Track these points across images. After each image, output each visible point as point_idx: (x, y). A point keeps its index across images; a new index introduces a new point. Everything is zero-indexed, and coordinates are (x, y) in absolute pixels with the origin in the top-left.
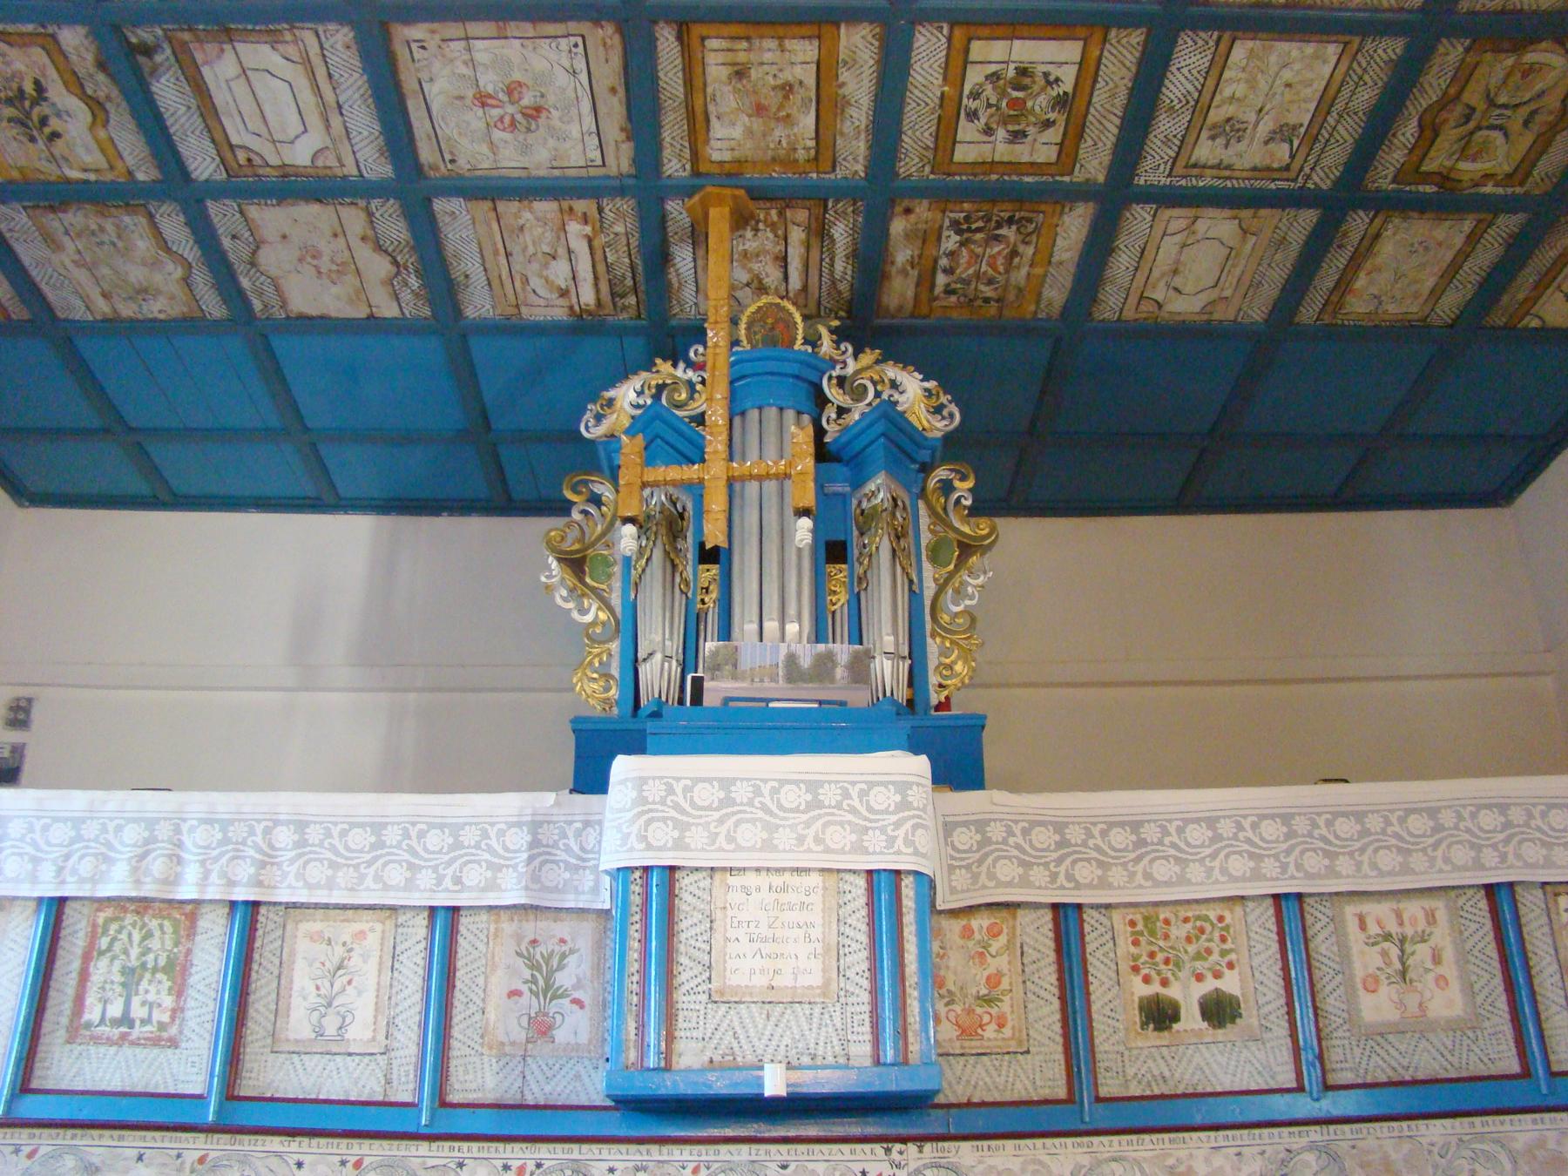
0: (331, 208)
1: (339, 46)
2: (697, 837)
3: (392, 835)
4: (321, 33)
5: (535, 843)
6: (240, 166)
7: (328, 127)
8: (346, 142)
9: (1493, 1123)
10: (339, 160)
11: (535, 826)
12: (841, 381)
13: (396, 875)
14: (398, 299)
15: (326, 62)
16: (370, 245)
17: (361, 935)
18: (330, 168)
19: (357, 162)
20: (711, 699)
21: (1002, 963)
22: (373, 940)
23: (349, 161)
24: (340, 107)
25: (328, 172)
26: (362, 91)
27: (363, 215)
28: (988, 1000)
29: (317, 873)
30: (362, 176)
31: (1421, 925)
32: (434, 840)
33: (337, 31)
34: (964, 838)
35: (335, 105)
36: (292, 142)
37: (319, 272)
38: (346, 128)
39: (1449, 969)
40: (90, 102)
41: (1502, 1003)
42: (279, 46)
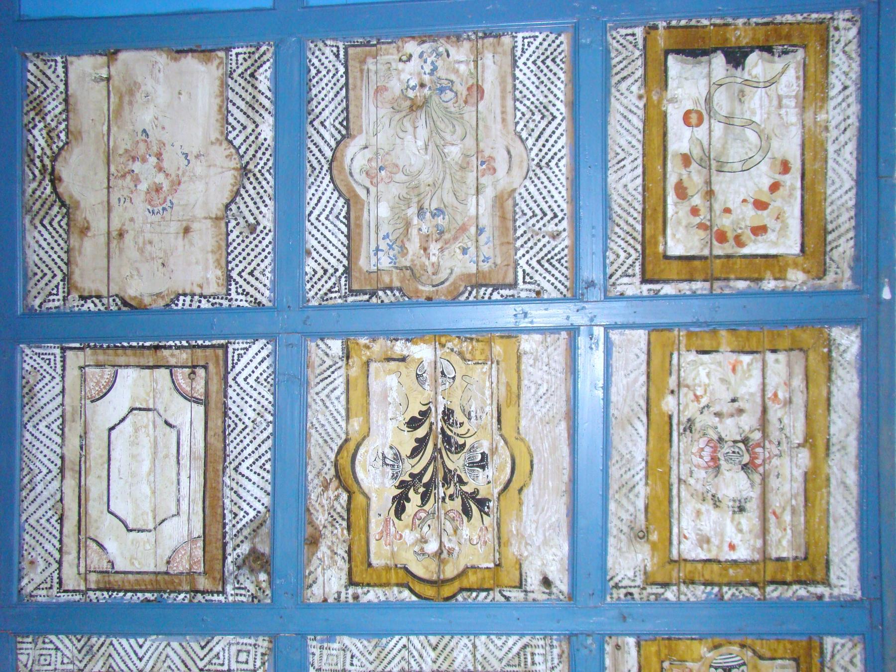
0: (114, 290)
1: (42, 565)
4: (56, 586)
6: (205, 367)
7: (84, 436)
8: (68, 408)
10: (84, 379)
14: (66, 101)
15: (61, 541)
16: (79, 216)
18: (99, 365)
19: (63, 377)
23: (73, 374)
24: (62, 470)
25: (101, 358)
26: (32, 495)
27: (76, 277)
30: (64, 350)
33: (37, 588)
35: (68, 474)
36: (132, 409)
37: (159, 156)
38: (63, 436)
40: (351, 481)
42: (105, 566)
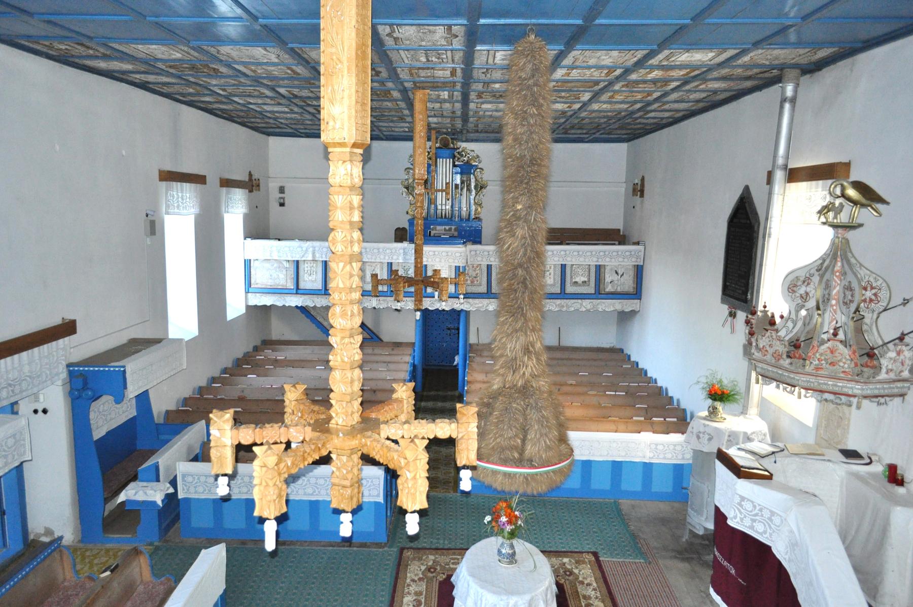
2: (430, 260)
3: (381, 250)
5: (404, 252)
9: (554, 300)
11: (404, 249)
12: (458, 153)
13: (382, 257)
17: (376, 265)
20: (432, 235)
21: (478, 271)
22: (379, 266)
28: (475, 277)
29: (369, 256)
31: (549, 268)
32: (388, 251)
34: (473, 253)
39: (552, 276)
41: (560, 282)
